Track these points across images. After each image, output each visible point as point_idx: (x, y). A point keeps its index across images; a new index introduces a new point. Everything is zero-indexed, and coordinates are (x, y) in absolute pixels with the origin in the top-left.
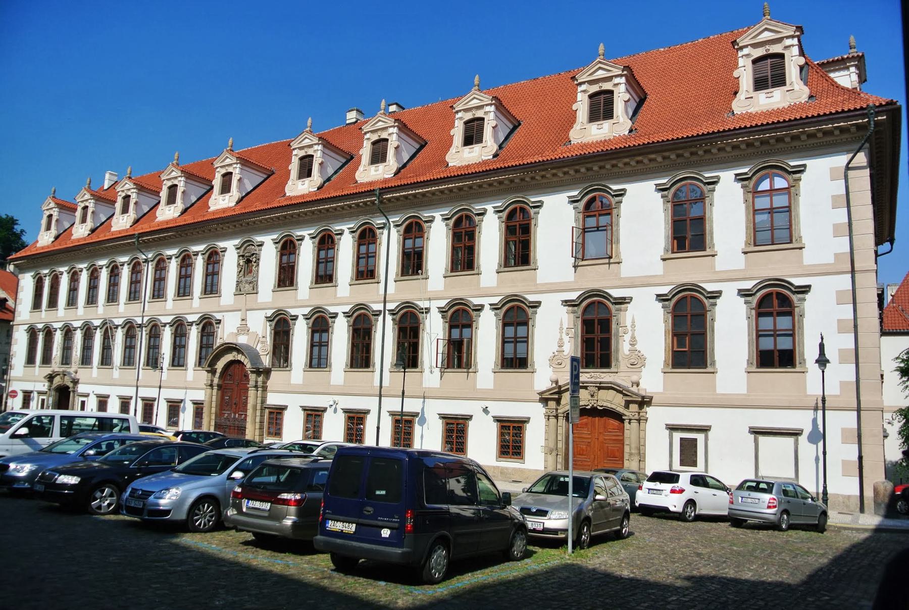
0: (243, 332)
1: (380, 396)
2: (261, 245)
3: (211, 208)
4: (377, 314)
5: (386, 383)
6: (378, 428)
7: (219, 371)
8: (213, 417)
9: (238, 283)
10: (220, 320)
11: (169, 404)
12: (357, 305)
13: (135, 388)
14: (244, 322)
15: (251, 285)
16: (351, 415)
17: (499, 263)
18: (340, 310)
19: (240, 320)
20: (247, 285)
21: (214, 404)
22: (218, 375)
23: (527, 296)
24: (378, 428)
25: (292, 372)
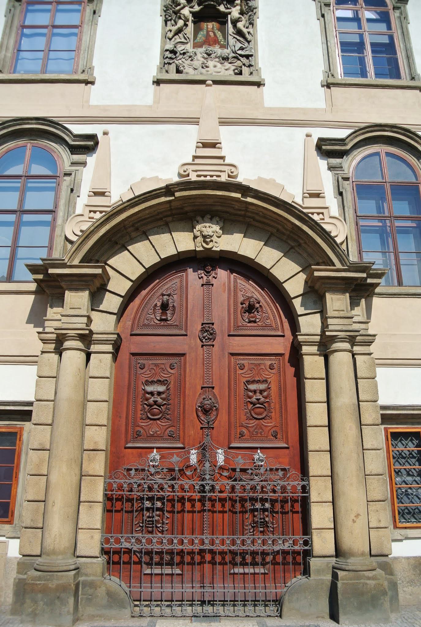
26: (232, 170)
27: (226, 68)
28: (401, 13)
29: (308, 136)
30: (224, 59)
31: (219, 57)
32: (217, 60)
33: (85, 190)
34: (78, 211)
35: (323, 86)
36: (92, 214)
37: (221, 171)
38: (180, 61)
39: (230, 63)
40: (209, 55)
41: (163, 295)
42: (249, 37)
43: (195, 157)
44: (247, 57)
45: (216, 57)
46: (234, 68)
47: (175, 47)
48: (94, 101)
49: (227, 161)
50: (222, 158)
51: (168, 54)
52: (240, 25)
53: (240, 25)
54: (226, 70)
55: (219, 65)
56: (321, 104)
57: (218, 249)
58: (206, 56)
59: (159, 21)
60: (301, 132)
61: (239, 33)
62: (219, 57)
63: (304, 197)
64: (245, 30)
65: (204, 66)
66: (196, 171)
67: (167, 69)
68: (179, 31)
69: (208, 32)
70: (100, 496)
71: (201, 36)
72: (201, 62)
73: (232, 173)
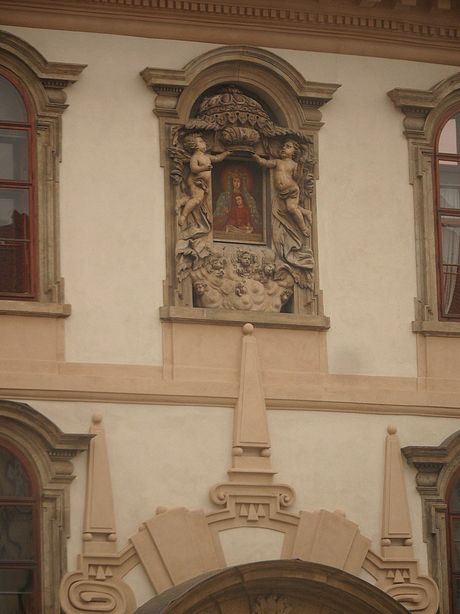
0: (253, 514)
15: (274, 285)
26: (287, 499)
27: (271, 292)
29: (391, 432)
30: (268, 275)
32: (258, 276)
34: (71, 568)
35: (415, 332)
37: (270, 497)
39: (277, 280)
40: (244, 266)
43: (231, 474)
44: (304, 271)
45: (257, 272)
46: (282, 290)
47: (191, 245)
49: (278, 480)
50: (271, 475)
51: (183, 264)
52: (293, 204)
54: (270, 295)
63: (384, 545)
64: (299, 212)
65: (240, 291)
66: (235, 496)
67: (181, 292)
69: (234, 195)
72: (234, 284)
73: (286, 502)
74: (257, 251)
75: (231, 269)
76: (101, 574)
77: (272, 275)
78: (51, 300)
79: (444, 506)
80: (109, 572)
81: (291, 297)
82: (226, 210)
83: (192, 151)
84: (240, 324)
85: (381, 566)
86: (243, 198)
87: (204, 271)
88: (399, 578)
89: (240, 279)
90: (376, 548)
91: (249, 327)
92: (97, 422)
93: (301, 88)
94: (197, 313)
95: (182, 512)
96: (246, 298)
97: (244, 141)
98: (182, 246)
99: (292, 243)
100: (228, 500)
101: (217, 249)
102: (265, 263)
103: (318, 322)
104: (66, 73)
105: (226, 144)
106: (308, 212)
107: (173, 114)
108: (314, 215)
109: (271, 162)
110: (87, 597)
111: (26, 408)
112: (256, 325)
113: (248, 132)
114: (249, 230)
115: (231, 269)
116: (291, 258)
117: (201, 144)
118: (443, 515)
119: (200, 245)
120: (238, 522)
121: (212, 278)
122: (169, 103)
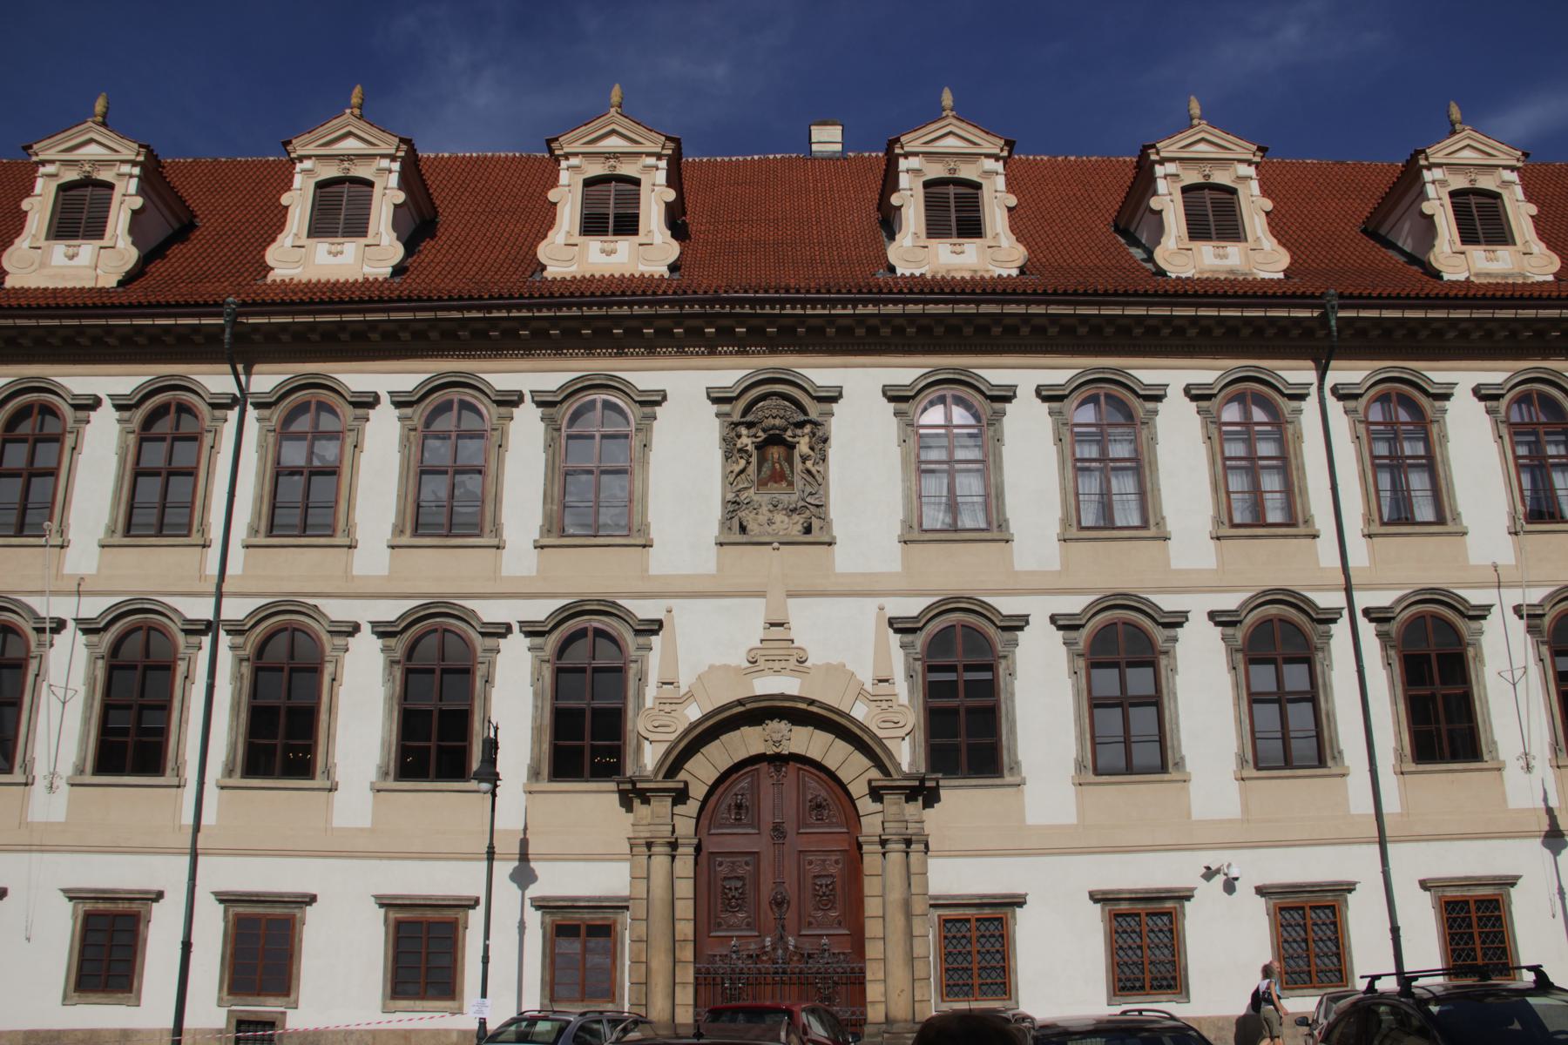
0: (777, 666)
1: (1382, 843)
2: (653, 401)
3: (549, 269)
4: (1329, 618)
5: (1391, 805)
6: (1395, 931)
7: (698, 791)
8: (687, 953)
9: (733, 507)
10: (660, 623)
11: (393, 915)
12: (1265, 593)
13: (187, 860)
14: (777, 632)
15: (796, 517)
16: (1290, 901)
17: (903, 522)
18: (1198, 606)
19: (760, 622)
20: (779, 517)
21: (685, 909)
22: (692, 807)
23: (1155, 598)
24: (1395, 931)
25: (1026, 788)
28: (995, 431)
29: (882, 609)
30: (793, 510)
31: (786, 509)
33: (653, 678)
34: (649, 703)
36: (662, 707)
38: (743, 513)
40: (775, 506)
41: (736, 795)
42: (820, 480)
45: (783, 509)
46: (802, 521)
47: (737, 496)
48: (654, 569)
49: (796, 645)
50: (792, 641)
51: (731, 507)
53: (809, 464)
55: (786, 519)
56: (896, 566)
57: (787, 753)
58: (771, 507)
59: (718, 455)
60: (872, 604)
61: (809, 472)
62: (786, 509)
64: (814, 470)
65: (770, 522)
68: (742, 471)
69: (773, 464)
70: (691, 979)
71: (766, 470)
72: (766, 518)
74: (785, 498)
75: (764, 509)
76: (667, 708)
77: (793, 510)
78: (640, 536)
79: (920, 656)
80: (674, 707)
81: (810, 524)
82: (769, 473)
83: (739, 436)
84: (769, 543)
85: (872, 698)
86: (780, 465)
87: (747, 512)
88: (884, 705)
89: (770, 515)
90: (868, 687)
91: (776, 545)
92: (669, 611)
93: (816, 391)
94: (744, 538)
95: (726, 667)
96: (774, 527)
97: (774, 427)
98: (730, 496)
99: (808, 489)
100: (757, 657)
101: (756, 498)
102: (789, 503)
103: (827, 539)
104: (652, 395)
105: (764, 431)
106: (821, 469)
107: (728, 415)
108: (827, 470)
109: (796, 439)
110: (656, 724)
111: (614, 603)
112: (781, 543)
113: (777, 422)
114: (784, 484)
115: (764, 509)
116: (808, 500)
117: (744, 431)
118: (920, 662)
119: (744, 496)
120: (767, 671)
121: (752, 515)
122: (726, 408)
